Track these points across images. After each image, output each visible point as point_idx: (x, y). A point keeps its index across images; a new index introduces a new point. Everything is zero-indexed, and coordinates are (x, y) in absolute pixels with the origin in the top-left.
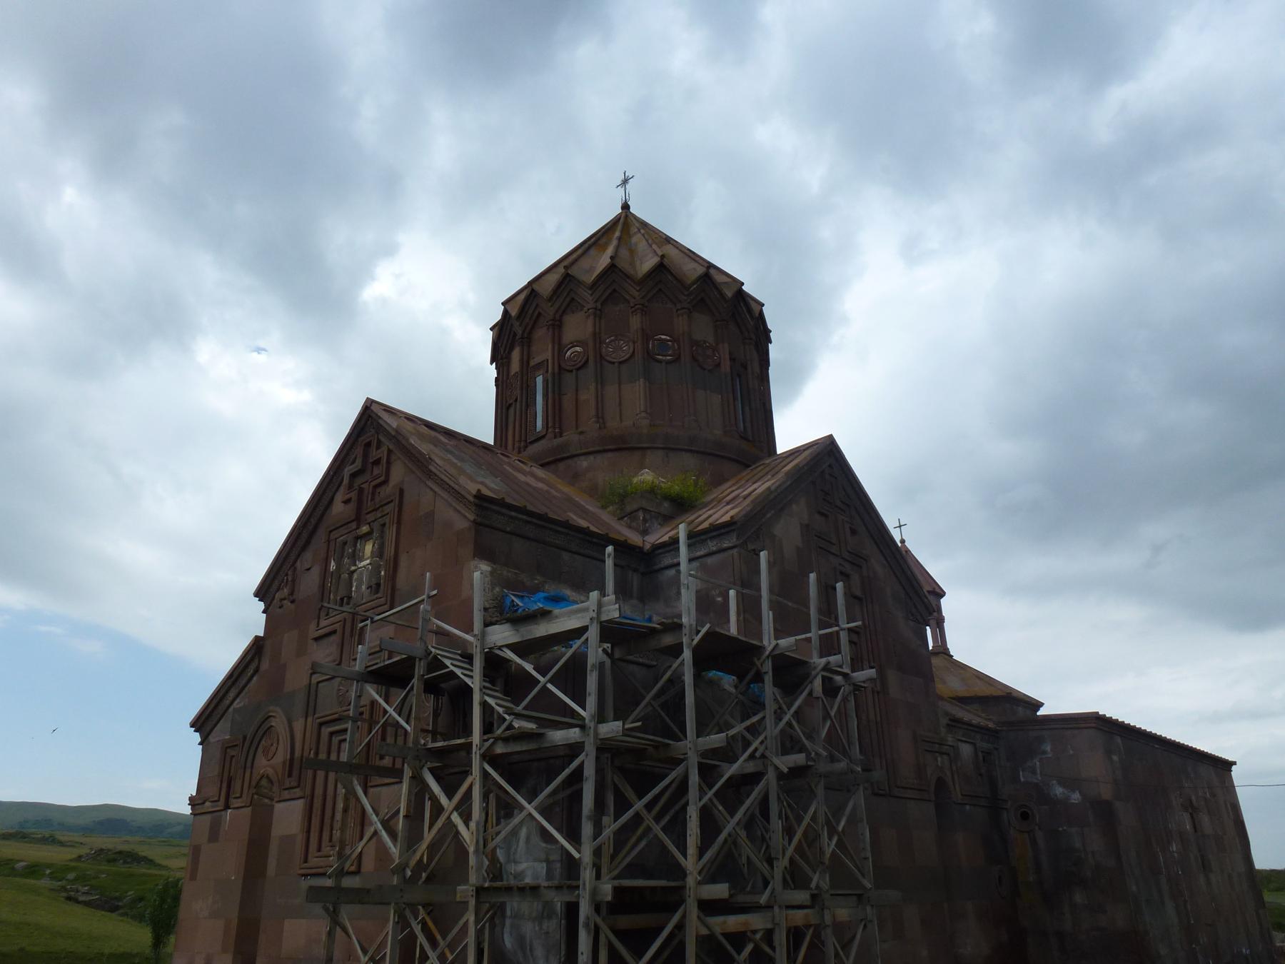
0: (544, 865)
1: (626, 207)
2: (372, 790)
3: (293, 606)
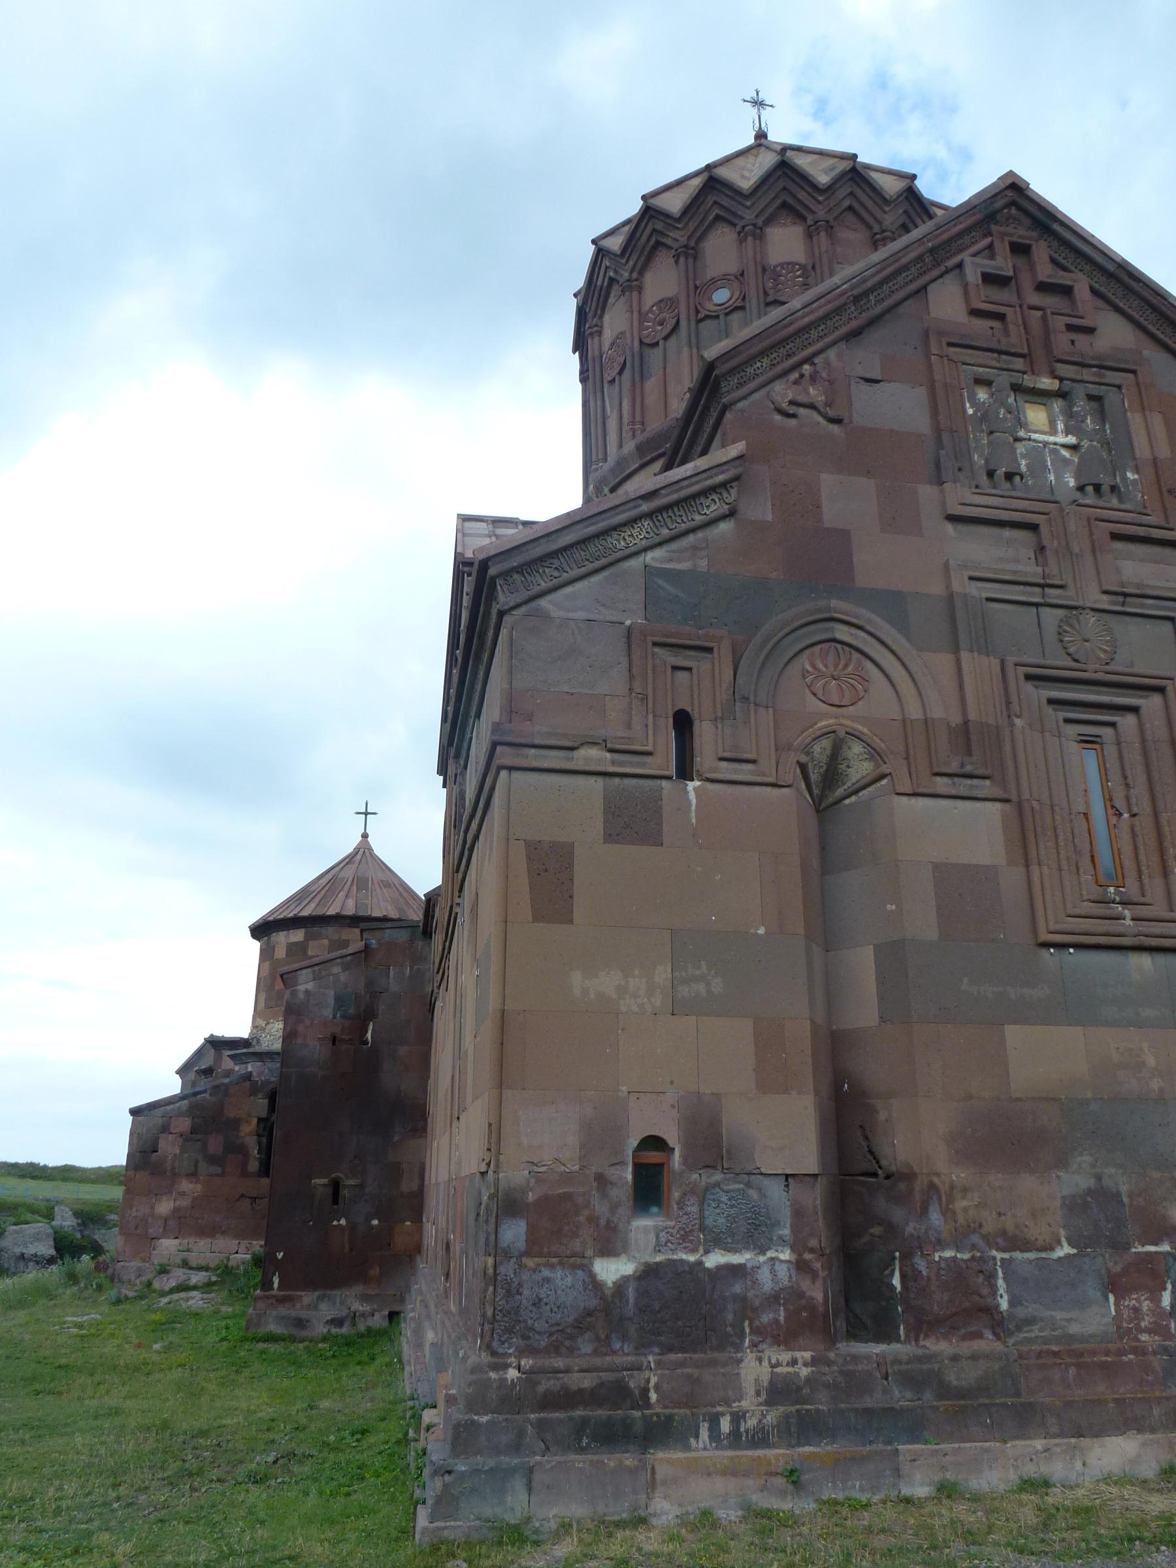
1: (761, 135)
3: (835, 429)
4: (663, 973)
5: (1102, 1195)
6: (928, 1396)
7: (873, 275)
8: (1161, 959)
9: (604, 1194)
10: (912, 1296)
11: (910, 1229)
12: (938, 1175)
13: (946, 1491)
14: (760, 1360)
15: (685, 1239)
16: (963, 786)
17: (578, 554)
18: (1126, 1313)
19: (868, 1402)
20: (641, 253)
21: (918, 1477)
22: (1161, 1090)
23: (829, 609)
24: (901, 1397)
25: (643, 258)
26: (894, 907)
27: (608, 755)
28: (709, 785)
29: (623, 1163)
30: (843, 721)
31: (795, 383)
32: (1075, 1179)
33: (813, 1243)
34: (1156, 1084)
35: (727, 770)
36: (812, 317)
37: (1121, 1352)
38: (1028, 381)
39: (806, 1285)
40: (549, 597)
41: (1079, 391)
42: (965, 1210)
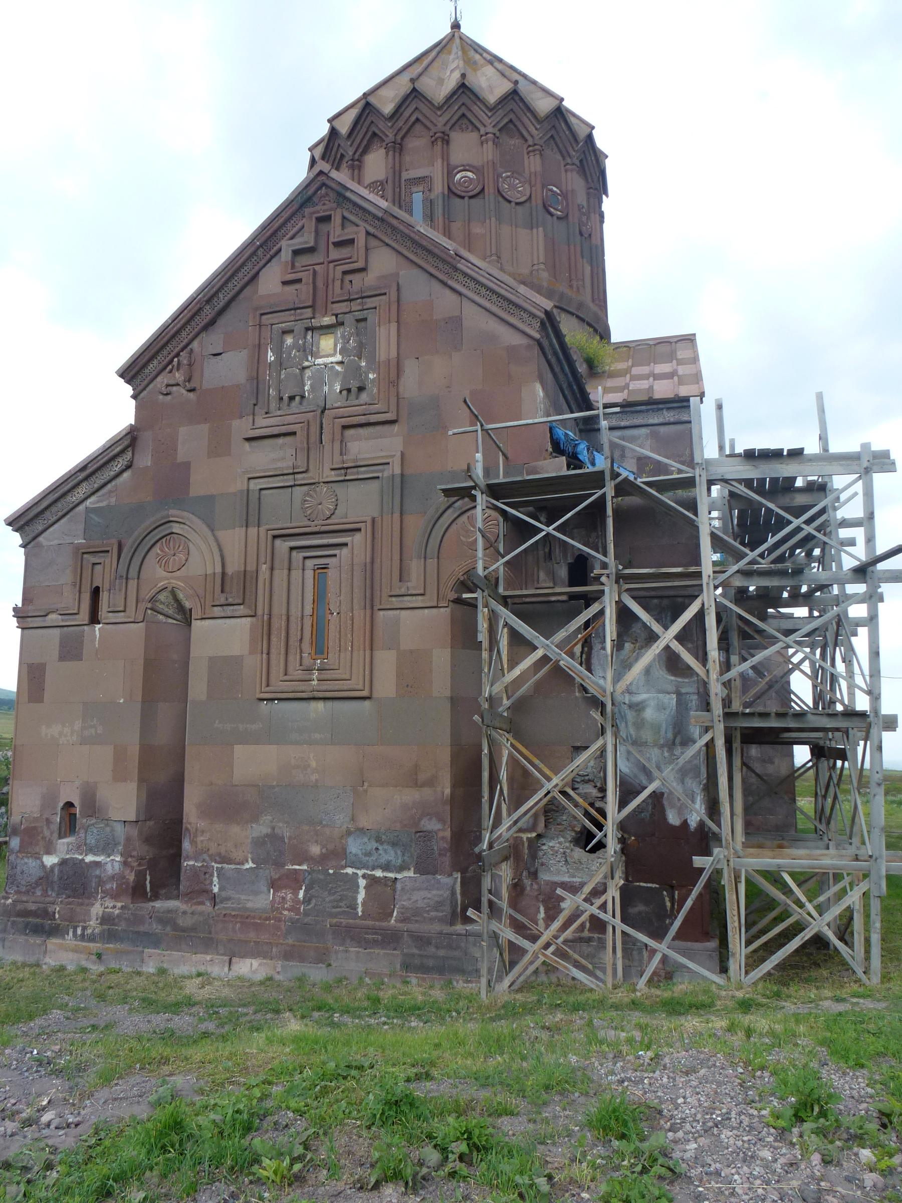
0: (674, 696)
1: (456, 26)
2: (382, 613)
3: (191, 395)
4: (78, 725)
5: (274, 837)
6: (168, 928)
7: (219, 281)
8: (329, 704)
9: (49, 828)
12: (190, 824)
13: (162, 972)
14: (102, 905)
15: (78, 848)
16: (229, 610)
17: (54, 509)
18: (277, 899)
19: (142, 929)
21: (151, 964)
22: (316, 780)
23: (168, 516)
24: (156, 928)
27: (60, 617)
28: (106, 626)
29: (56, 814)
30: (172, 581)
31: (171, 372)
32: (260, 829)
33: (134, 853)
34: (314, 777)
35: (112, 618)
36: (179, 326)
37: (268, 919)
38: (315, 323)
39: (127, 872)
40: (43, 535)
41: (349, 319)
42: (202, 841)
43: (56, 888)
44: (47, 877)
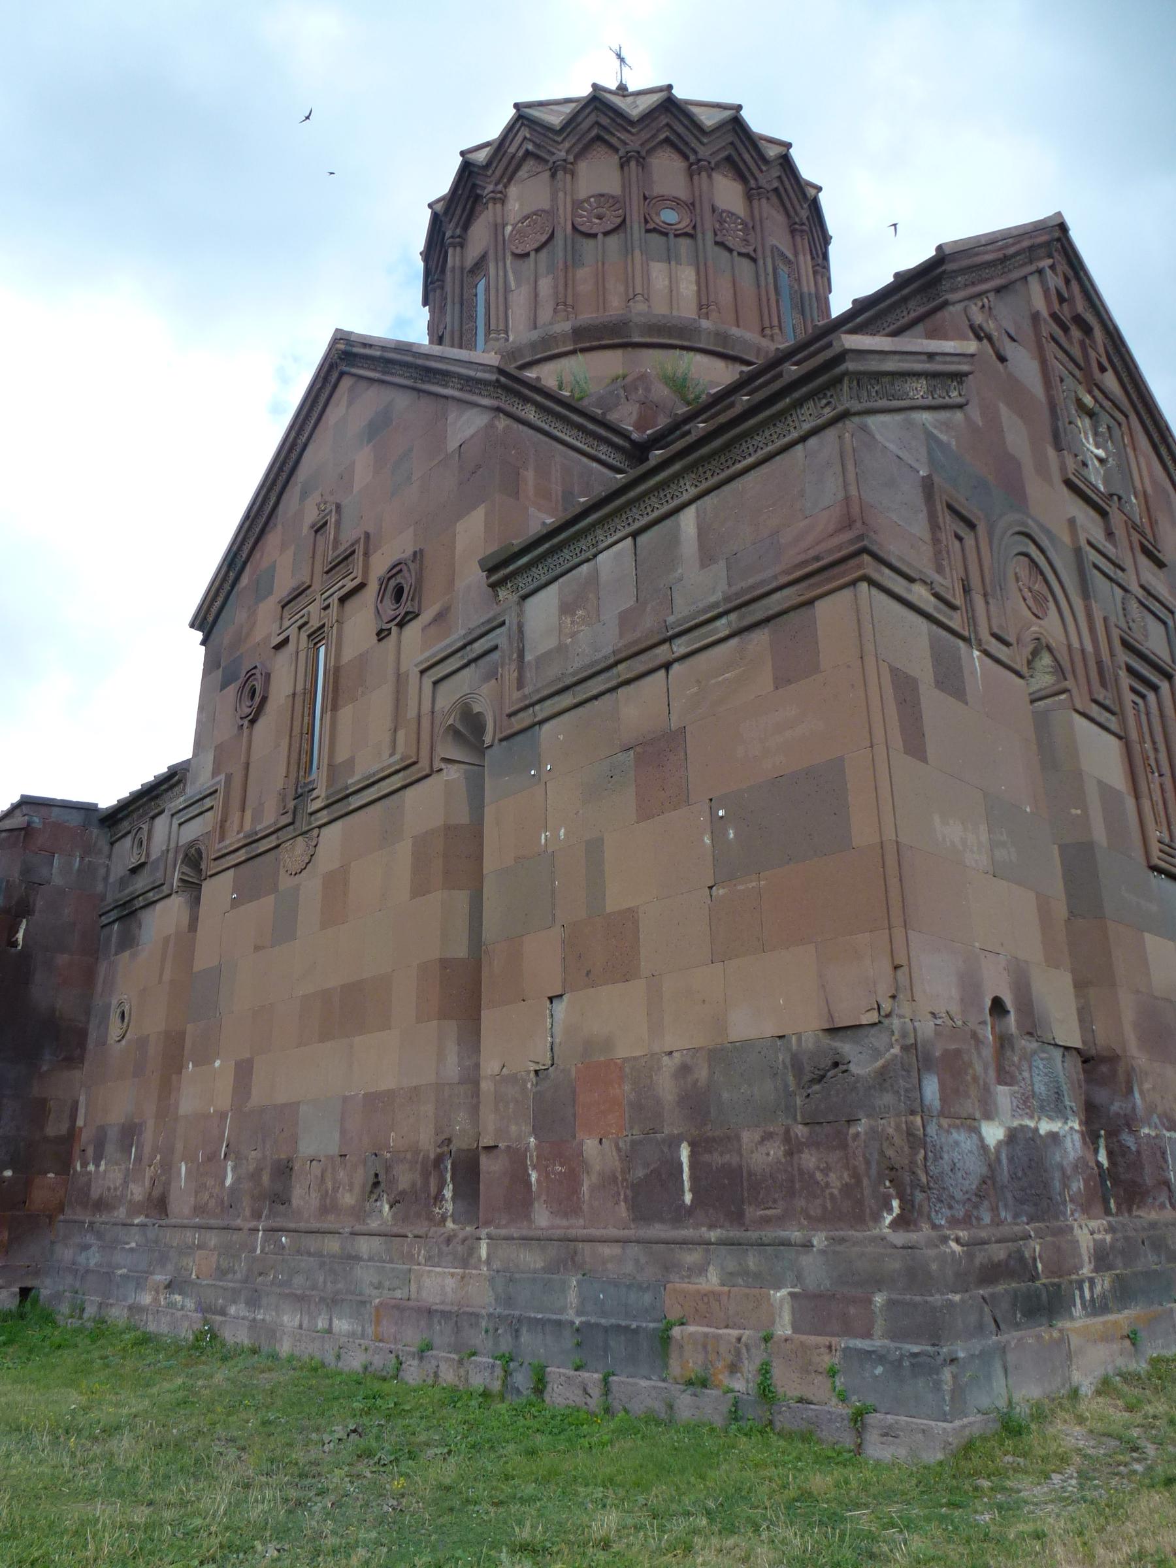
9: (979, 1054)
10: (1121, 1170)
11: (1115, 1107)
20: (579, 140)
25: (580, 146)
26: (1079, 812)
27: (932, 599)
43: (1010, 1201)
44: (992, 1178)
